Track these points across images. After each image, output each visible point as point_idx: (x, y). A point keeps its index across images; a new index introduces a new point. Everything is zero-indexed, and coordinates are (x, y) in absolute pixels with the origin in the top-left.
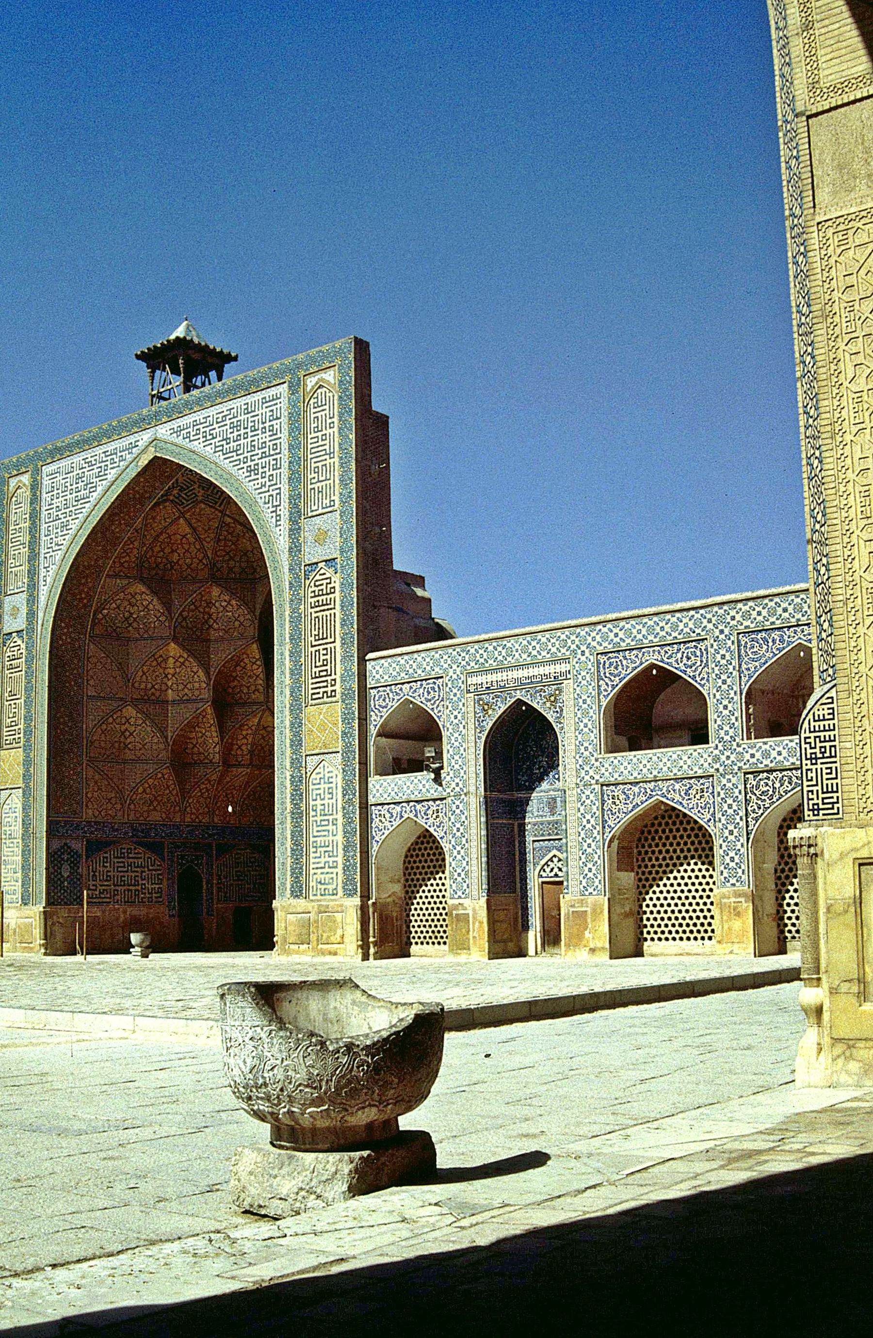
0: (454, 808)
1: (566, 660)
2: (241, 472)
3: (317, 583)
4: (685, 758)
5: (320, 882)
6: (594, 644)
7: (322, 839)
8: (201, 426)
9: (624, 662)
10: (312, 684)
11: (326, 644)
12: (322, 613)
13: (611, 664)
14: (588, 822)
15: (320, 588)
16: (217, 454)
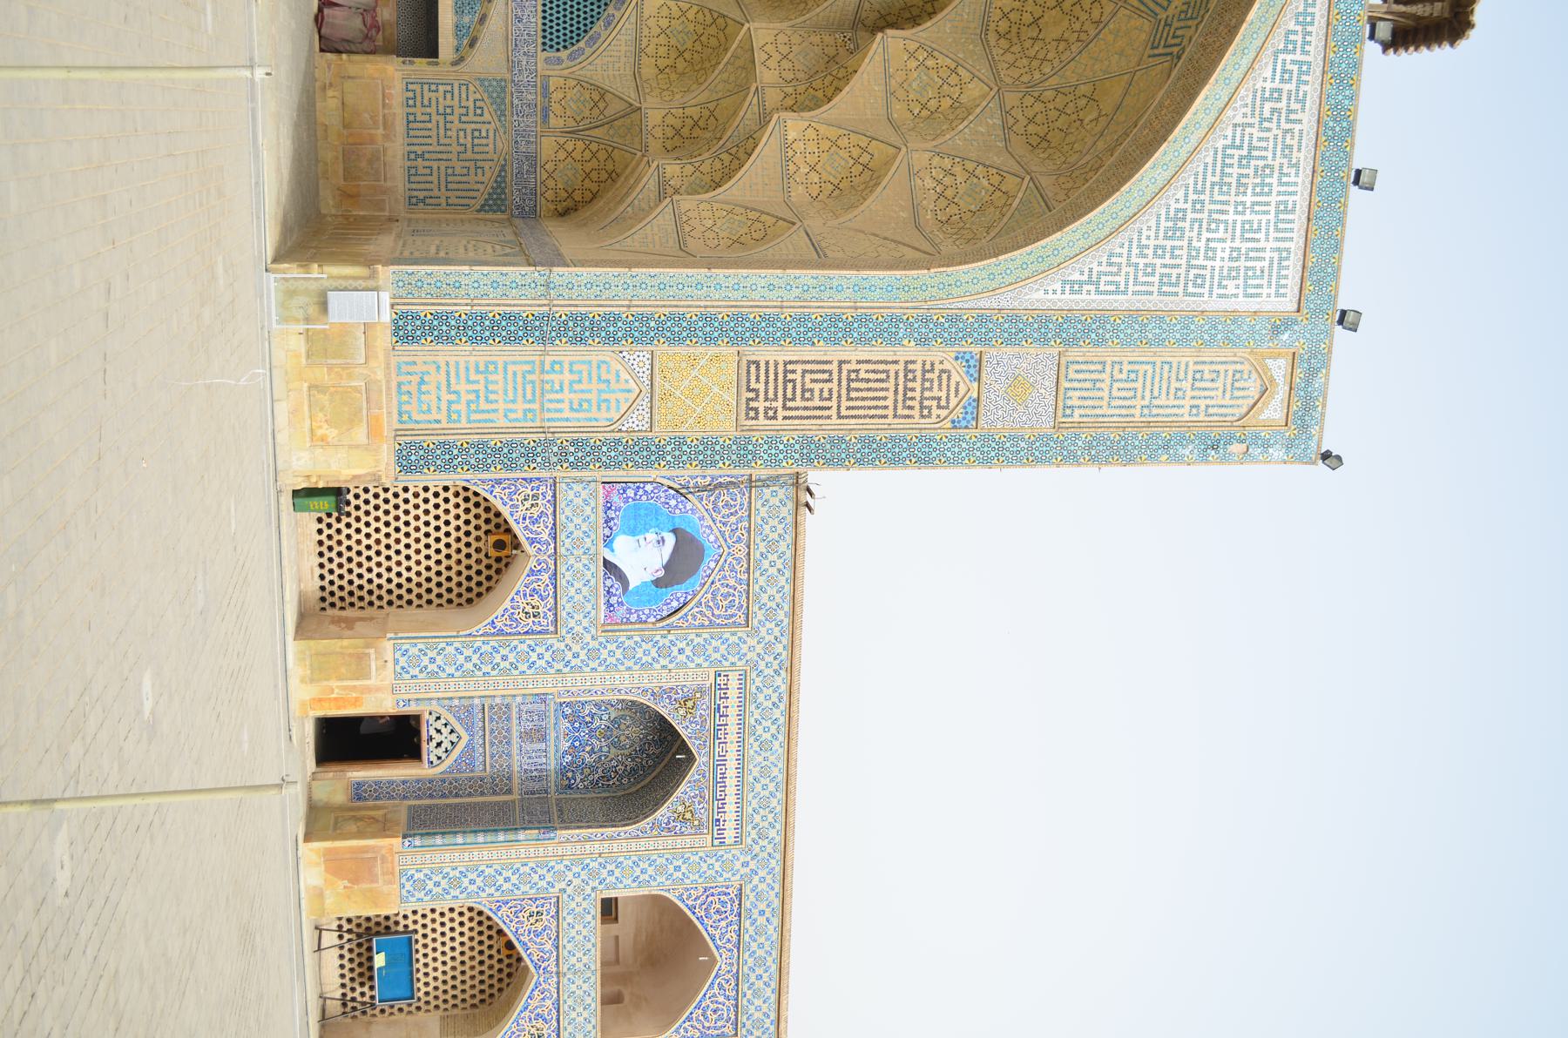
0: (539, 650)
1: (739, 840)
2: (1180, 195)
3: (944, 376)
4: (585, 1014)
5: (422, 382)
6: (756, 880)
7: (499, 387)
8: (1292, 86)
9: (723, 924)
10: (776, 364)
11: (839, 396)
12: (892, 389)
13: (723, 903)
14: (507, 880)
15: (936, 384)
16: (1229, 133)
